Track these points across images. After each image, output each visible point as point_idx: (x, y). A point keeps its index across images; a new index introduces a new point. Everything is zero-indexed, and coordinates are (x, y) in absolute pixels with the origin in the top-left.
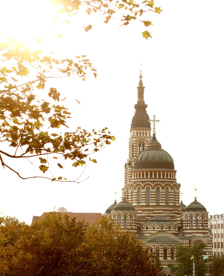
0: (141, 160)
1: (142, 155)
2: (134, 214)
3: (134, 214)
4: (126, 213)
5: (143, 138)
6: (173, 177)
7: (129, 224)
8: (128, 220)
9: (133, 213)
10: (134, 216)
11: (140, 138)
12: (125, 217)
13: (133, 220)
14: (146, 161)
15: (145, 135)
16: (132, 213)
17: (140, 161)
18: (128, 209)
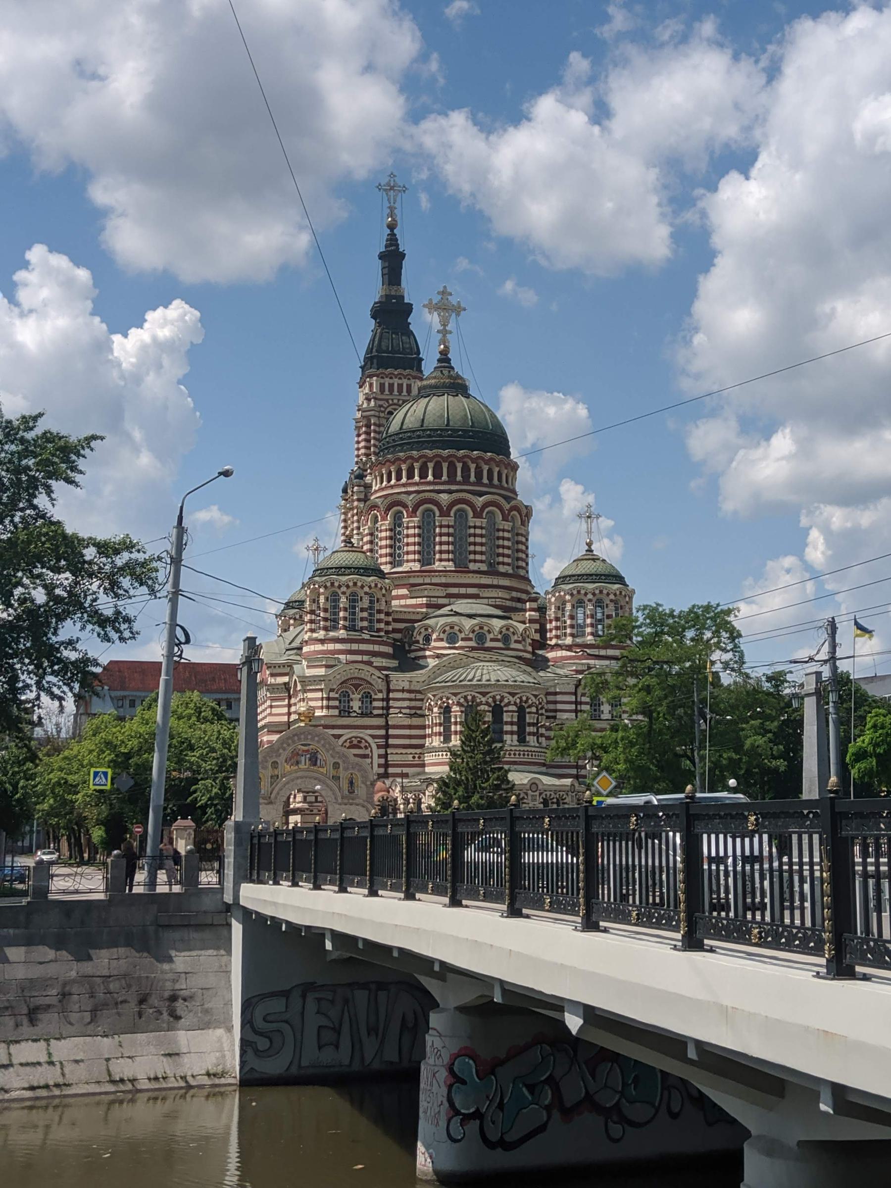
0: (404, 427)
1: (407, 412)
2: (384, 591)
3: (384, 591)
4: (355, 584)
5: (399, 400)
6: (500, 479)
7: (365, 624)
8: (362, 610)
9: (379, 586)
10: (384, 595)
11: (390, 402)
12: (354, 601)
13: (379, 612)
14: (422, 426)
15: (405, 393)
16: (376, 585)
17: (401, 429)
18: (362, 571)
